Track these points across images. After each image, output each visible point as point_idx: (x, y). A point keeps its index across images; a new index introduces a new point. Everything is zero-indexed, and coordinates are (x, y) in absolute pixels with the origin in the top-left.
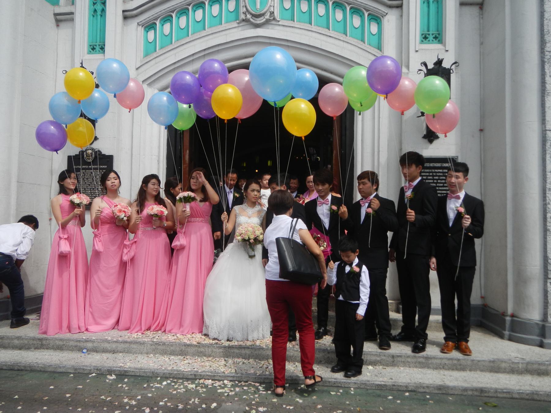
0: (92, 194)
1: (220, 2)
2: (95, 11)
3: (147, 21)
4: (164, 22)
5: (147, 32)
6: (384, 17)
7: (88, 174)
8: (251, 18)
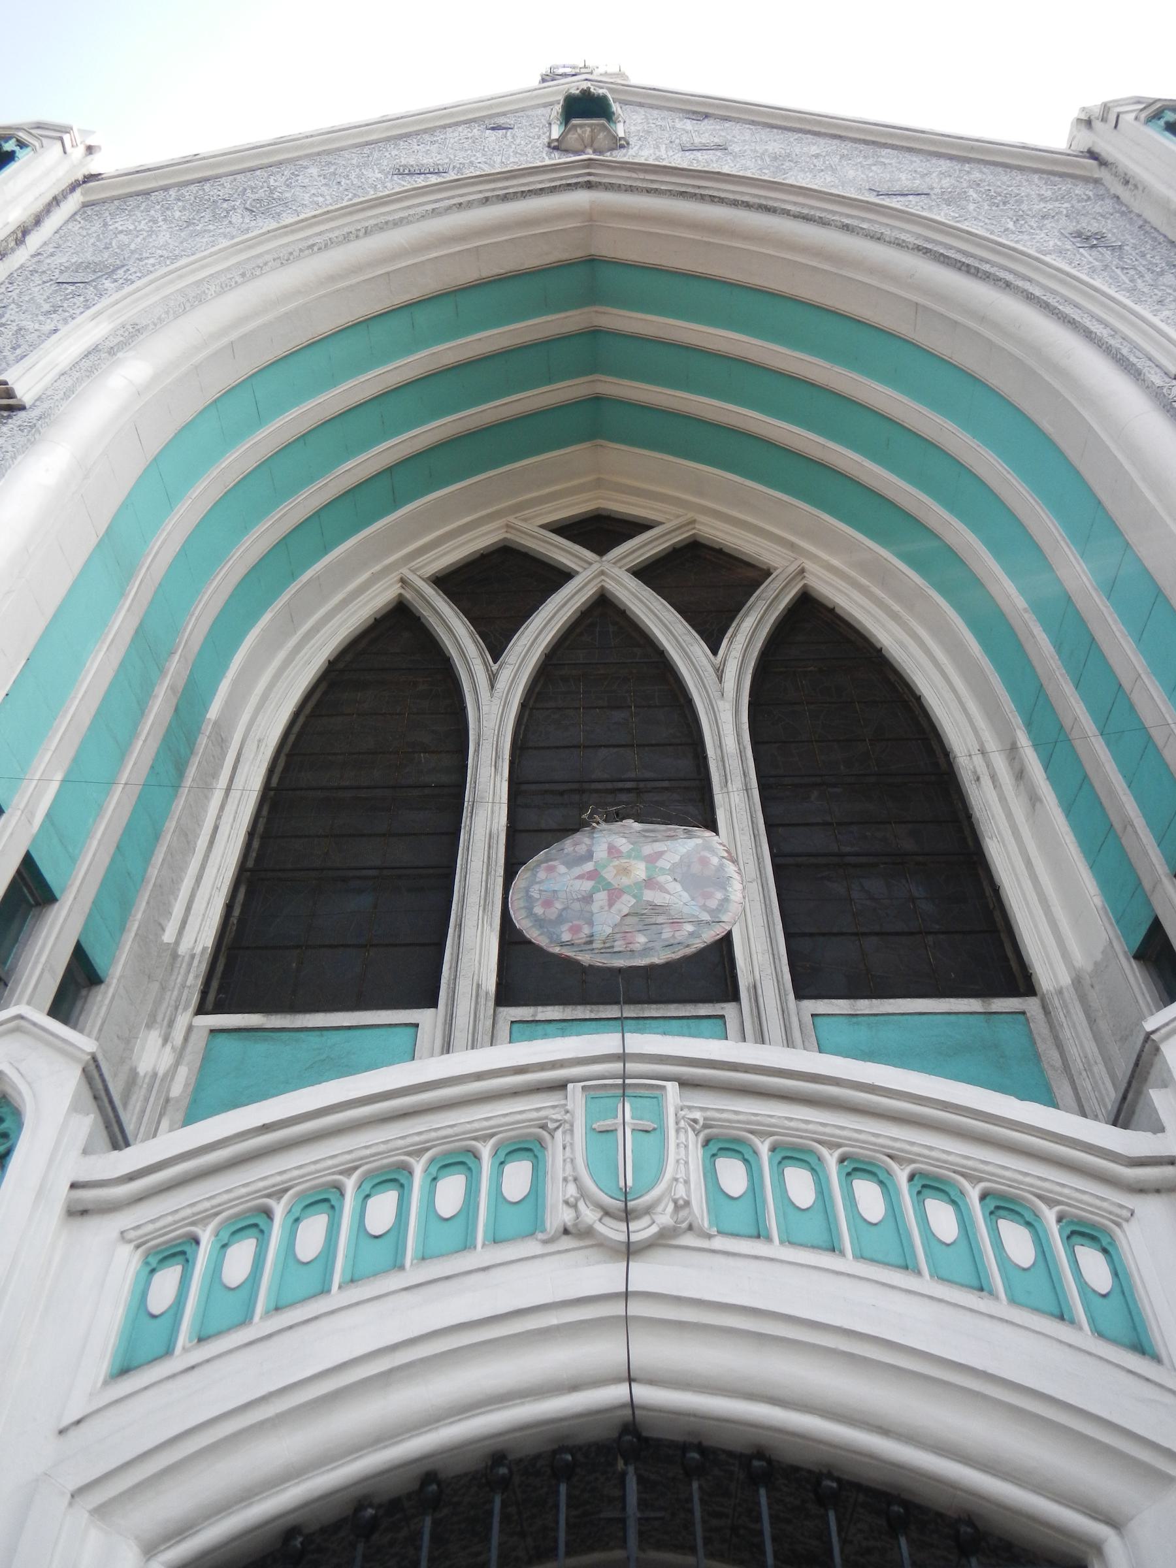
1: (470, 1169)
3: (165, 1227)
4: (234, 1233)
5: (153, 1271)
6: (1125, 1225)
8: (600, 1220)
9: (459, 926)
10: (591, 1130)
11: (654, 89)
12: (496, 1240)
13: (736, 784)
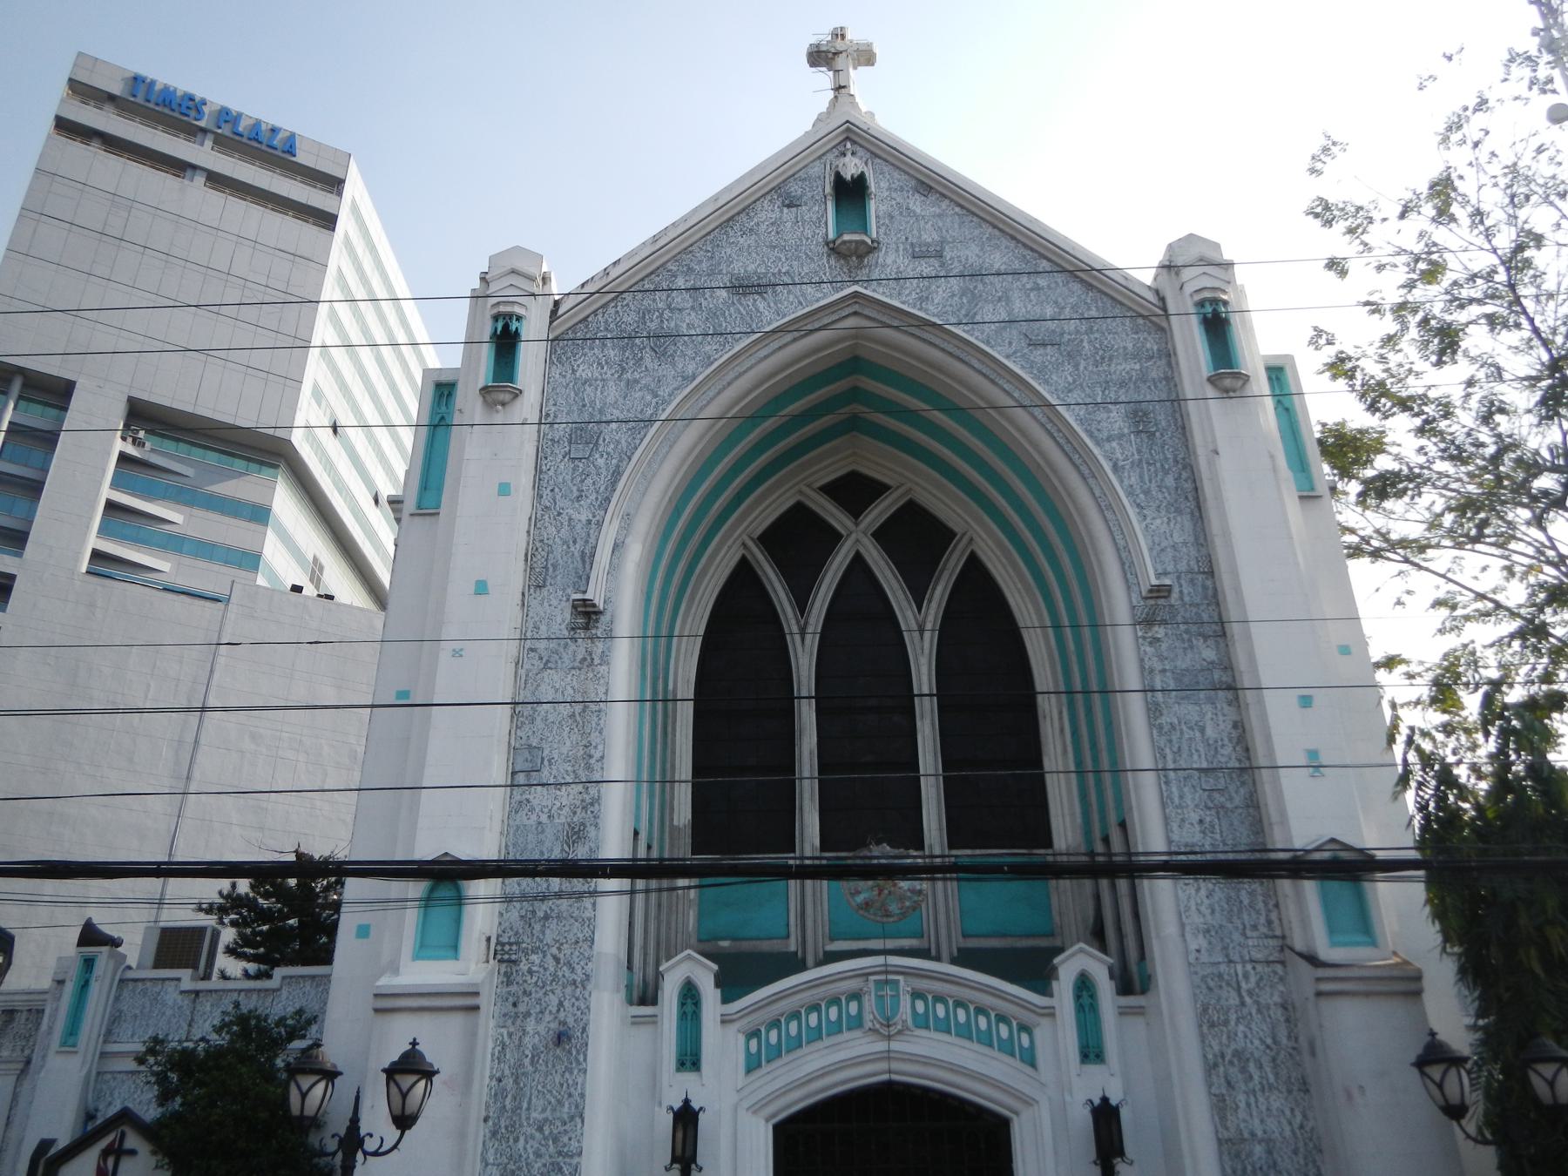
2: (685, 1013)
9: (801, 809)
10: (876, 995)
11: (895, 149)
12: (849, 1029)
13: (927, 721)
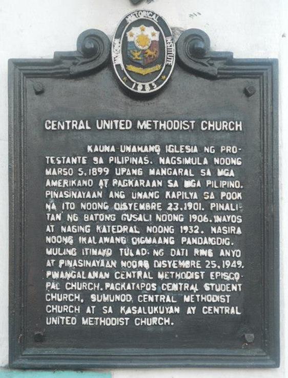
0: (159, 282)
7: (129, 165)
